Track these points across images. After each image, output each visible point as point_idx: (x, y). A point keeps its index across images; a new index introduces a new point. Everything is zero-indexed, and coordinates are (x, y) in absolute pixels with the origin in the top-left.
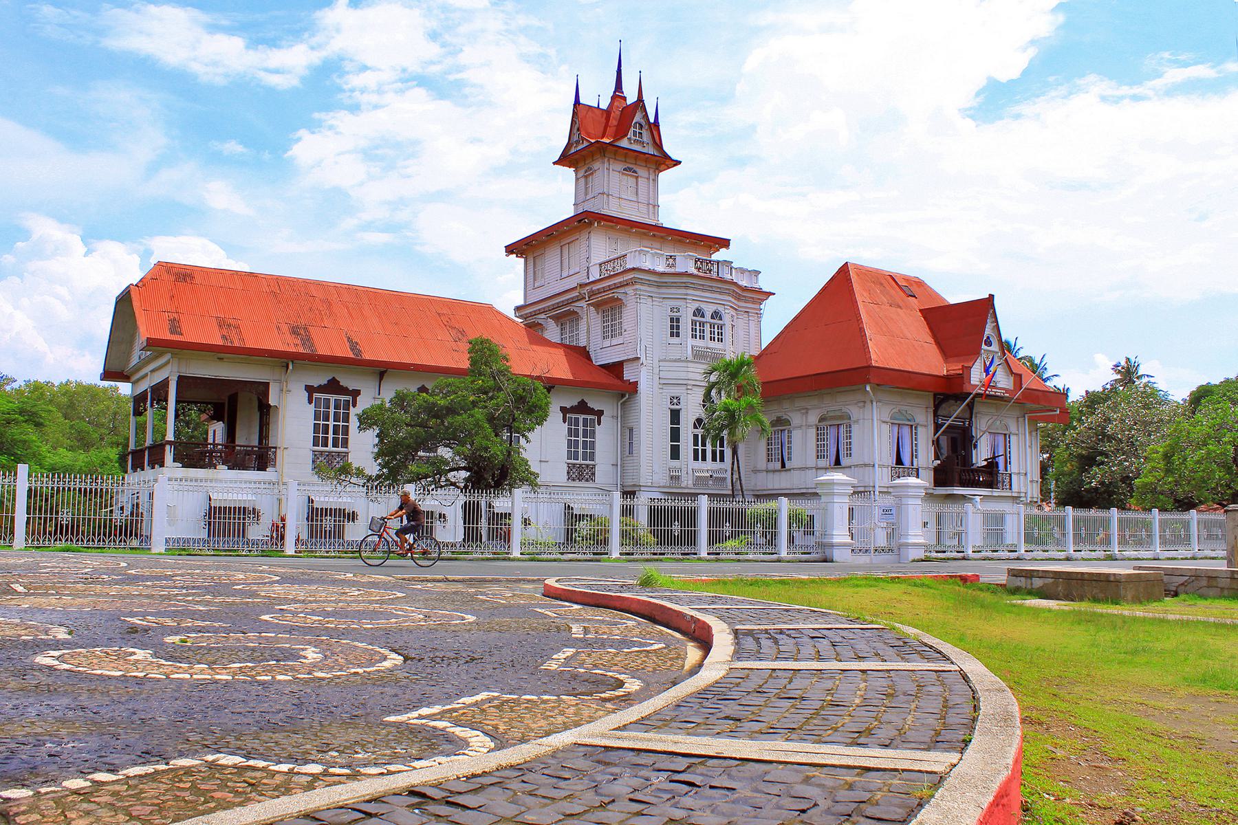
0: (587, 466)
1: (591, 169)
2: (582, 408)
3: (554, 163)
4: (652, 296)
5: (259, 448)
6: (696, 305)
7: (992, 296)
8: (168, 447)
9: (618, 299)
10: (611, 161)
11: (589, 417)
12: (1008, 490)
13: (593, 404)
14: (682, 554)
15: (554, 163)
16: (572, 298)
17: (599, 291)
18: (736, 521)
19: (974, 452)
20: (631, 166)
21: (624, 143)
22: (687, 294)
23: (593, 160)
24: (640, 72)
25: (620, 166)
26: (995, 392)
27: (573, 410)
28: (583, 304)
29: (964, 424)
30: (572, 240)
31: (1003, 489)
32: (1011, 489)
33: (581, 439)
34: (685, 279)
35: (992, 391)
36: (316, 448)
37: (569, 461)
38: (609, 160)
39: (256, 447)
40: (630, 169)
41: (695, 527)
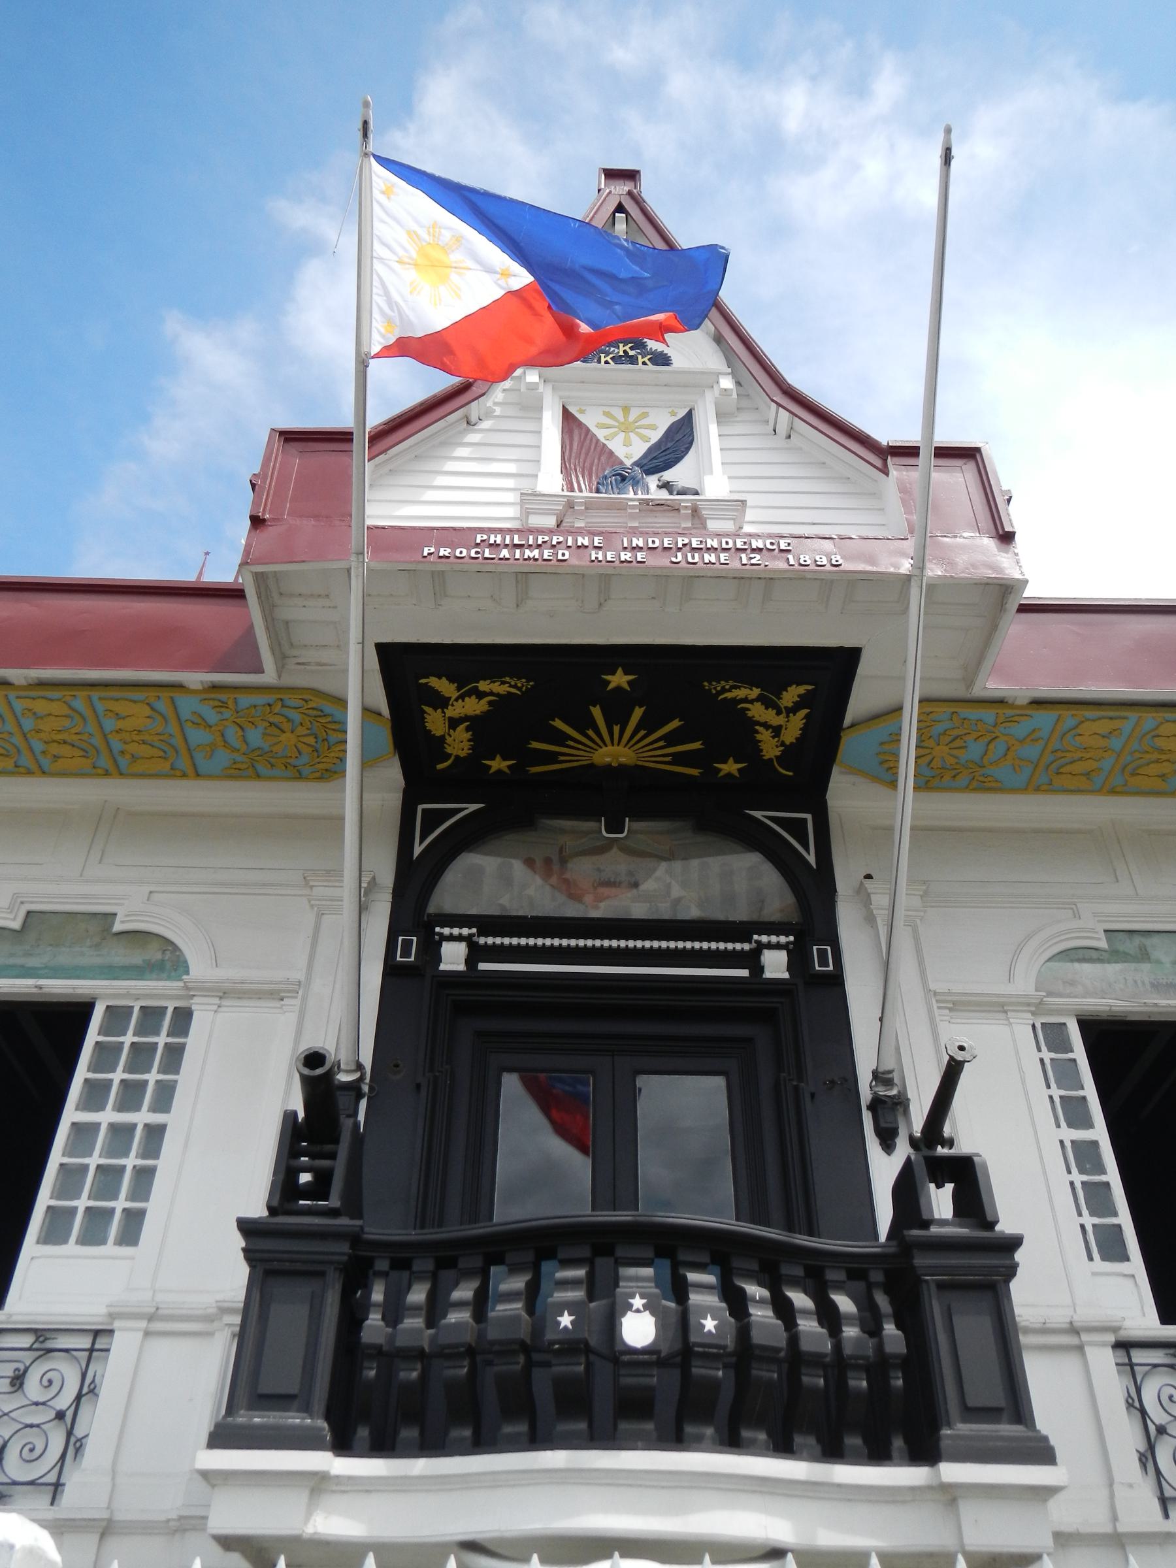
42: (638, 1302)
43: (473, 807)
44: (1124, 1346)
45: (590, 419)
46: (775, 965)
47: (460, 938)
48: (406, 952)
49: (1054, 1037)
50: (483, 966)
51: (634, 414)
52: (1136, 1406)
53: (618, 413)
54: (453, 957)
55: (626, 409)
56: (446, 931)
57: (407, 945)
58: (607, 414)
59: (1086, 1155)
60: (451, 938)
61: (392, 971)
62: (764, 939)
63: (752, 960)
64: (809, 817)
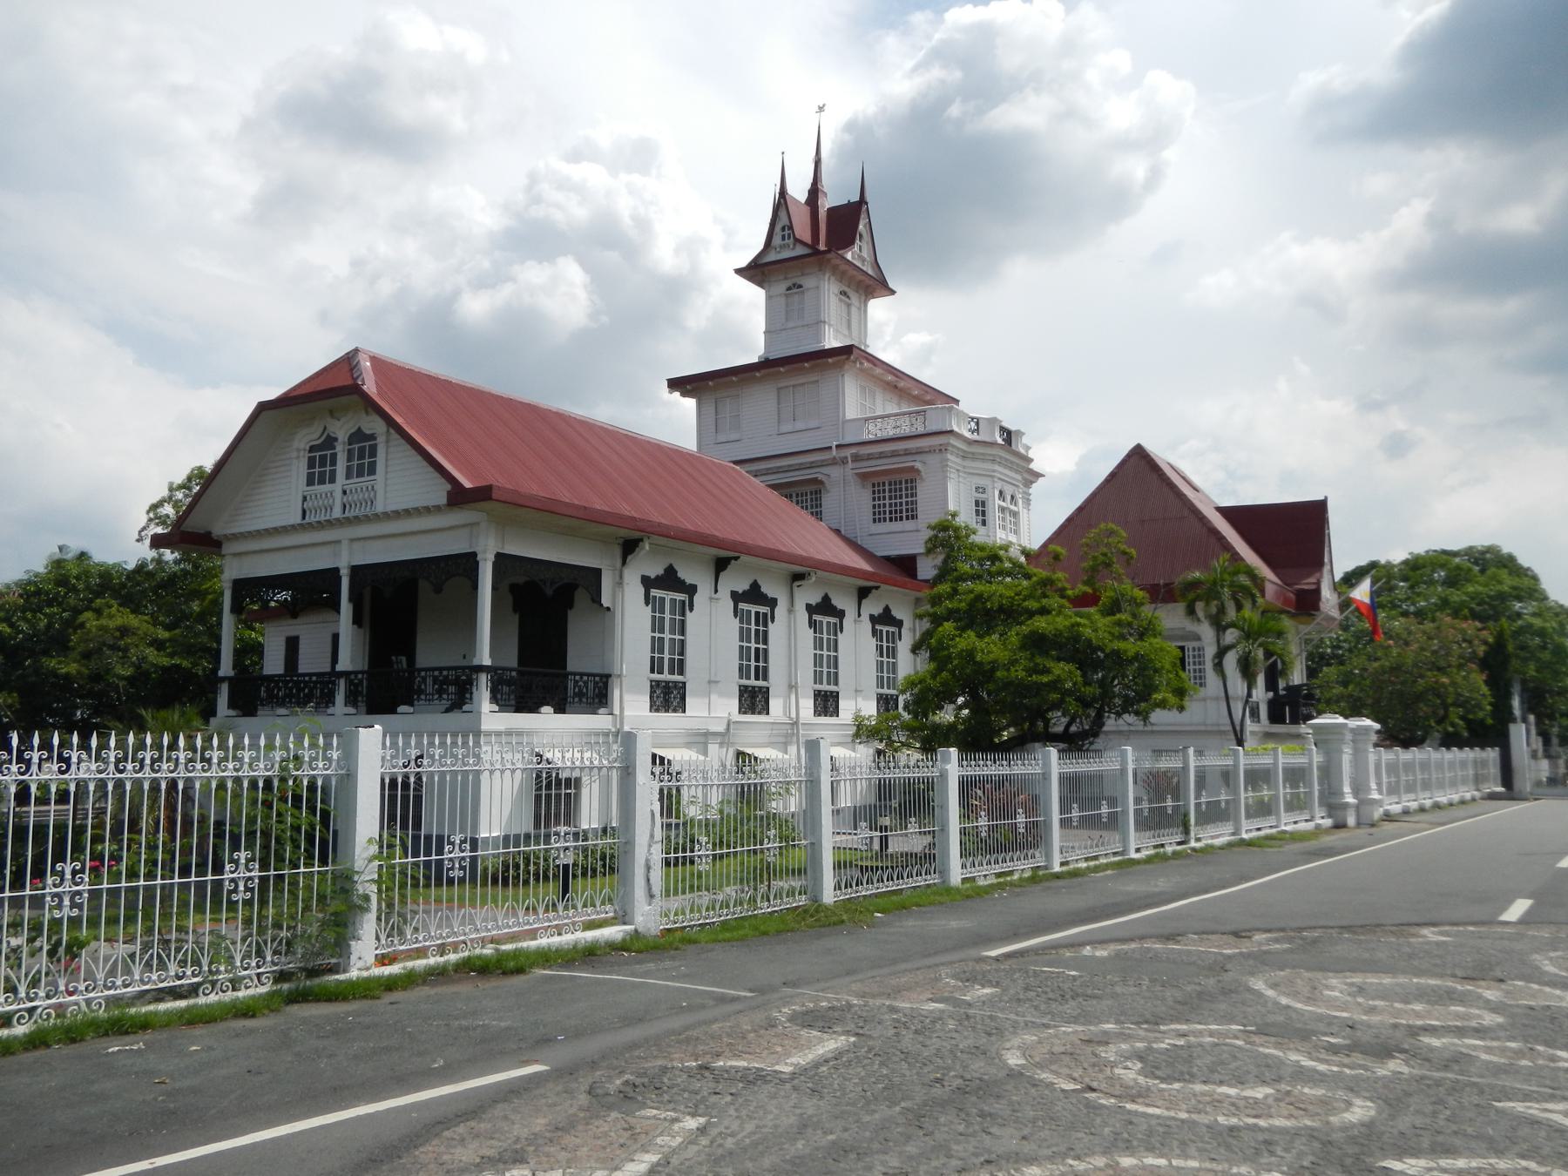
1: (800, 286)
3: (739, 271)
4: (958, 470)
5: (519, 672)
6: (999, 485)
7: (1326, 498)
8: (483, 679)
9: (918, 471)
10: (832, 278)
15: (739, 271)
16: (823, 461)
17: (870, 457)
20: (846, 289)
21: (849, 256)
22: (994, 471)
23: (803, 275)
28: (835, 472)
30: (801, 381)
34: (989, 451)
36: (656, 676)
38: (829, 279)
39: (511, 670)
40: (843, 293)
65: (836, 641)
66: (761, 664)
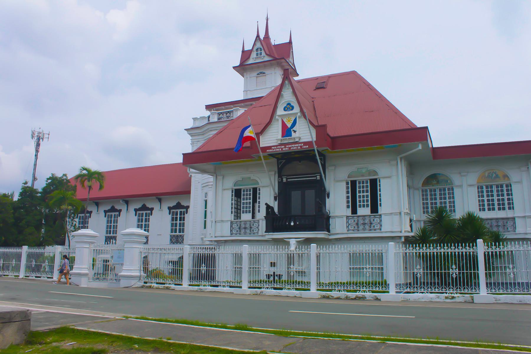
0: (181, 235)
2: (179, 206)
11: (182, 210)
12: (379, 231)
13: (184, 204)
14: (36, 277)
18: (437, 265)
19: (327, 200)
21: (251, 61)
24: (258, 22)
25: (255, 74)
26: (290, 148)
27: (174, 207)
29: (317, 178)
31: (370, 230)
32: (381, 229)
33: (178, 222)
35: (285, 147)
37: (172, 234)
40: (261, 73)
41: (214, 268)
42: (292, 222)
43: (284, 161)
44: (347, 217)
45: (285, 120)
46: (318, 178)
47: (285, 178)
48: (280, 180)
49: (347, 183)
50: (288, 180)
51: (290, 119)
52: (347, 222)
53: (288, 119)
54: (284, 180)
55: (289, 118)
56: (283, 177)
57: (280, 179)
58: (287, 119)
59: (348, 197)
60: (284, 178)
61: (279, 182)
62: (317, 175)
63: (316, 176)
64: (322, 157)
65: (117, 220)
66: (109, 230)
